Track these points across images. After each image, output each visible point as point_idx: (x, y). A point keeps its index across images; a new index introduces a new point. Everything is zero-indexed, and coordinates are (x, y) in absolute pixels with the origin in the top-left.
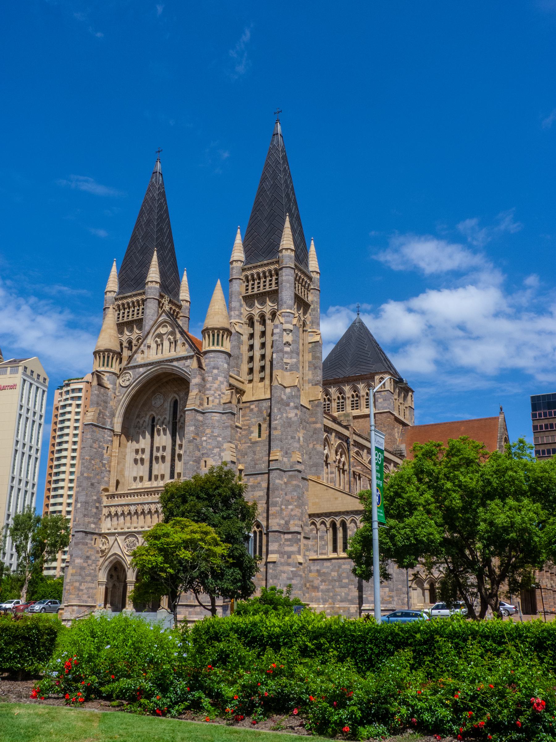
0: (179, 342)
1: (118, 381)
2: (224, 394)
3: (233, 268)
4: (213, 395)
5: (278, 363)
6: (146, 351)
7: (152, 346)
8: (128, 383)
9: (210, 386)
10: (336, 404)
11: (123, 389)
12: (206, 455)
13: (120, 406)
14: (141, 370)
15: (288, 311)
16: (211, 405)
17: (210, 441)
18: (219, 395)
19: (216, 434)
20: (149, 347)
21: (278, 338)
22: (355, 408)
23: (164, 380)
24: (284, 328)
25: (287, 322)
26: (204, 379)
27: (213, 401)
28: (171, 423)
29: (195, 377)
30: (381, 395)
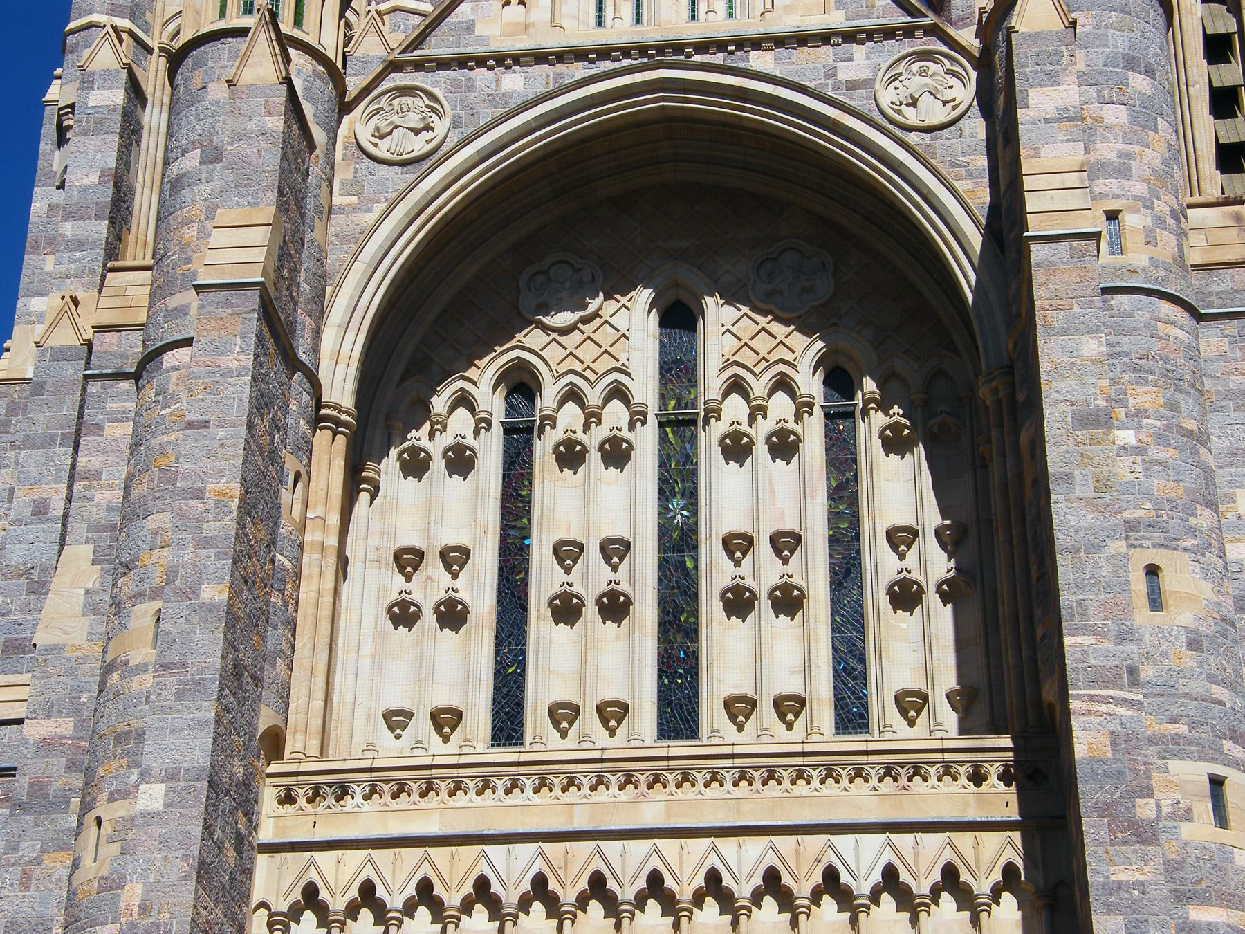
1: (343, 132)
8: (419, 146)
9: (1121, 154)
11: (382, 170)
12: (1157, 536)
13: (359, 268)
14: (515, 82)
17: (1167, 454)
18: (1174, 215)
19: (1191, 425)
28: (652, 421)
29: (1052, 79)
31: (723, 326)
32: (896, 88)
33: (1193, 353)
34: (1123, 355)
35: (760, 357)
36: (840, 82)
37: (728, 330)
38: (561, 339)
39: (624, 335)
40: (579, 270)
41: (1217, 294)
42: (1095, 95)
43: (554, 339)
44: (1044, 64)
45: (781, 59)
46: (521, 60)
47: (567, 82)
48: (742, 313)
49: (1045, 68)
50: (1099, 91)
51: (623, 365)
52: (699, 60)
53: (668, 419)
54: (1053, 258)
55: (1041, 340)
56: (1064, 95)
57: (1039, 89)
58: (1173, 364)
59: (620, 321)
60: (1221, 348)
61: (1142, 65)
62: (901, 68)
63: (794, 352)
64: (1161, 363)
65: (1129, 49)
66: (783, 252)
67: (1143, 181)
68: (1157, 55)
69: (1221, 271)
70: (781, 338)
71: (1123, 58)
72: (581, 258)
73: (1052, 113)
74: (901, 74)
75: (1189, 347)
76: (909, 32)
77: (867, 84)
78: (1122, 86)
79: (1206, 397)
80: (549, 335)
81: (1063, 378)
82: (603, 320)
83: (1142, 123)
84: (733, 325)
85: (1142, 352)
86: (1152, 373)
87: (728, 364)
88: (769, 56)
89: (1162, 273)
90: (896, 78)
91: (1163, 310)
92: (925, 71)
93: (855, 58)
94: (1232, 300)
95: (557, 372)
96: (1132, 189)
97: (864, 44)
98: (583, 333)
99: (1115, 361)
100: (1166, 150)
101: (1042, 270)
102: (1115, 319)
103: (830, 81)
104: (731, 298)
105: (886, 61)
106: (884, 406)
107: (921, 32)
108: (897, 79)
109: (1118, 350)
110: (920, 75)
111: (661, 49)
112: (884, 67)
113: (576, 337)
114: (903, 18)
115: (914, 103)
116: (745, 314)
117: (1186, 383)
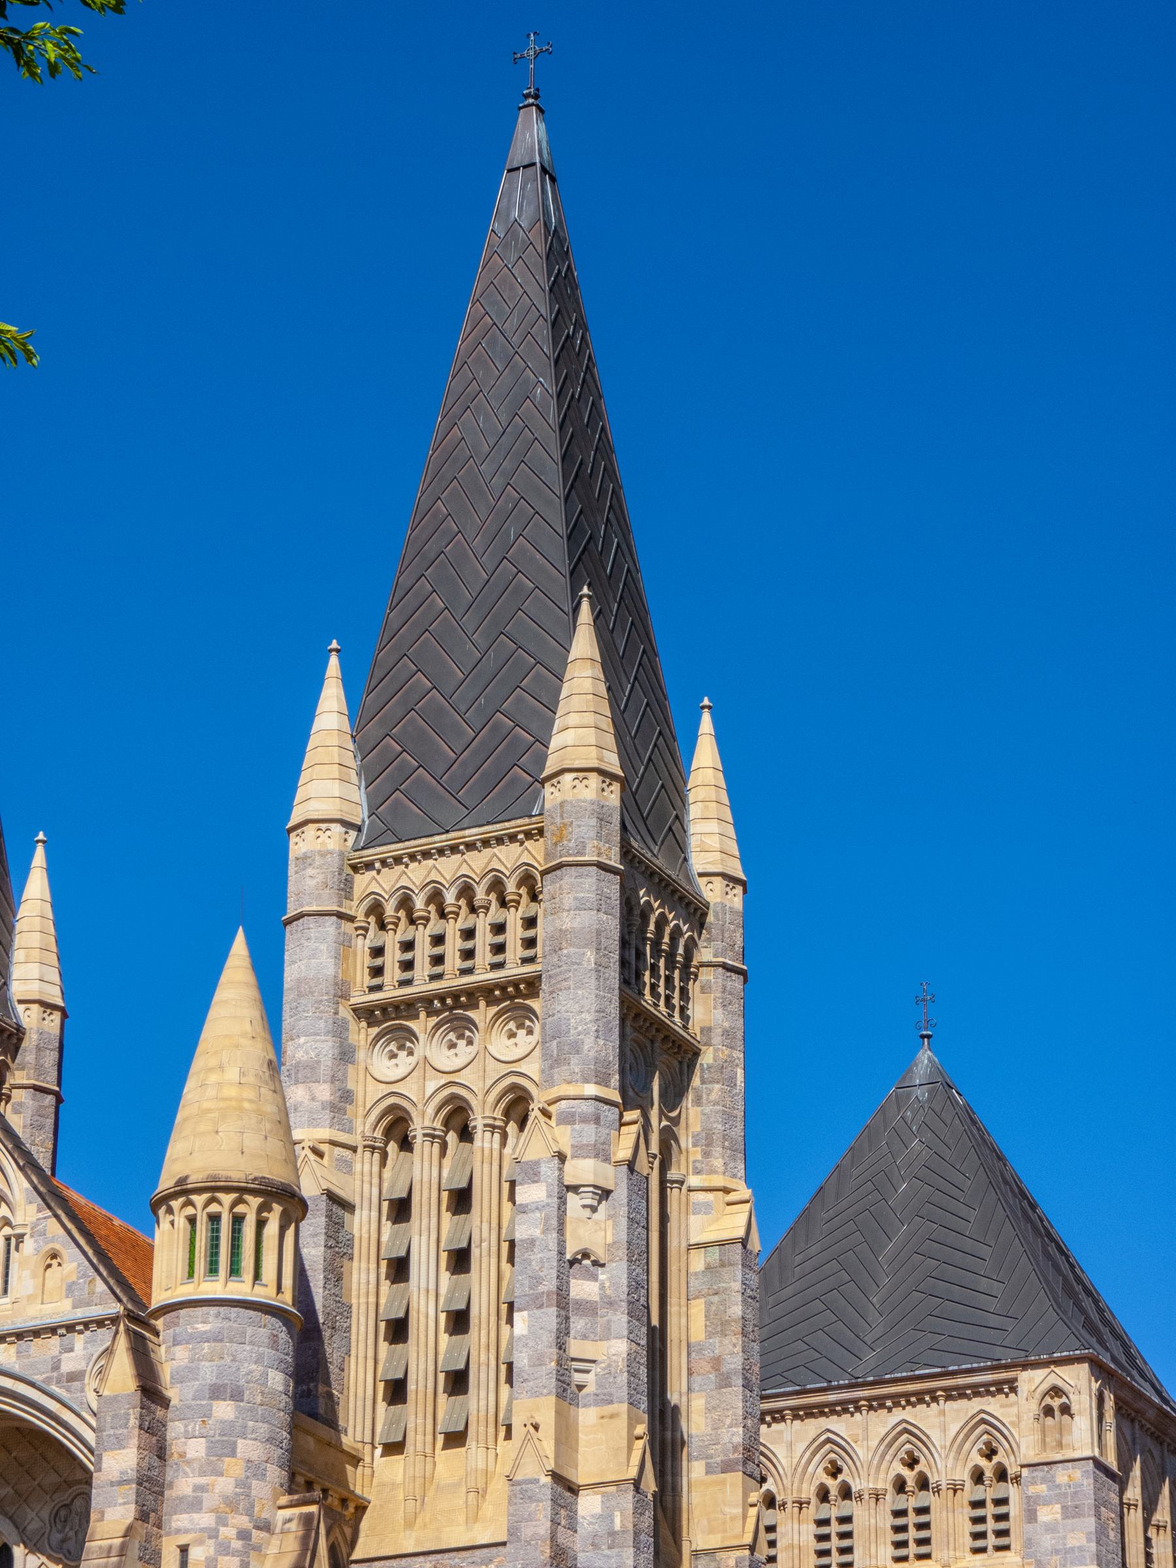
0: (28, 1245)
2: (266, 1527)
3: (304, 859)
5: (538, 1361)
9: (198, 1488)
10: (811, 1529)
15: (591, 1089)
18: (244, 1535)
21: (537, 1232)
22: (913, 1549)
25: (581, 1151)
26: (161, 1452)
29: (120, 1444)
30: (1050, 1481)
42: (182, 1430)
45: (21, 1353)
50: (186, 1426)
56: (126, 1459)
61: (229, 1391)
67: (212, 1511)
73: (115, 1476)
78: (207, 1415)
88: (13, 1349)
93: (76, 1348)
103: (55, 1374)
104: (34, 1547)
105: (96, 1351)
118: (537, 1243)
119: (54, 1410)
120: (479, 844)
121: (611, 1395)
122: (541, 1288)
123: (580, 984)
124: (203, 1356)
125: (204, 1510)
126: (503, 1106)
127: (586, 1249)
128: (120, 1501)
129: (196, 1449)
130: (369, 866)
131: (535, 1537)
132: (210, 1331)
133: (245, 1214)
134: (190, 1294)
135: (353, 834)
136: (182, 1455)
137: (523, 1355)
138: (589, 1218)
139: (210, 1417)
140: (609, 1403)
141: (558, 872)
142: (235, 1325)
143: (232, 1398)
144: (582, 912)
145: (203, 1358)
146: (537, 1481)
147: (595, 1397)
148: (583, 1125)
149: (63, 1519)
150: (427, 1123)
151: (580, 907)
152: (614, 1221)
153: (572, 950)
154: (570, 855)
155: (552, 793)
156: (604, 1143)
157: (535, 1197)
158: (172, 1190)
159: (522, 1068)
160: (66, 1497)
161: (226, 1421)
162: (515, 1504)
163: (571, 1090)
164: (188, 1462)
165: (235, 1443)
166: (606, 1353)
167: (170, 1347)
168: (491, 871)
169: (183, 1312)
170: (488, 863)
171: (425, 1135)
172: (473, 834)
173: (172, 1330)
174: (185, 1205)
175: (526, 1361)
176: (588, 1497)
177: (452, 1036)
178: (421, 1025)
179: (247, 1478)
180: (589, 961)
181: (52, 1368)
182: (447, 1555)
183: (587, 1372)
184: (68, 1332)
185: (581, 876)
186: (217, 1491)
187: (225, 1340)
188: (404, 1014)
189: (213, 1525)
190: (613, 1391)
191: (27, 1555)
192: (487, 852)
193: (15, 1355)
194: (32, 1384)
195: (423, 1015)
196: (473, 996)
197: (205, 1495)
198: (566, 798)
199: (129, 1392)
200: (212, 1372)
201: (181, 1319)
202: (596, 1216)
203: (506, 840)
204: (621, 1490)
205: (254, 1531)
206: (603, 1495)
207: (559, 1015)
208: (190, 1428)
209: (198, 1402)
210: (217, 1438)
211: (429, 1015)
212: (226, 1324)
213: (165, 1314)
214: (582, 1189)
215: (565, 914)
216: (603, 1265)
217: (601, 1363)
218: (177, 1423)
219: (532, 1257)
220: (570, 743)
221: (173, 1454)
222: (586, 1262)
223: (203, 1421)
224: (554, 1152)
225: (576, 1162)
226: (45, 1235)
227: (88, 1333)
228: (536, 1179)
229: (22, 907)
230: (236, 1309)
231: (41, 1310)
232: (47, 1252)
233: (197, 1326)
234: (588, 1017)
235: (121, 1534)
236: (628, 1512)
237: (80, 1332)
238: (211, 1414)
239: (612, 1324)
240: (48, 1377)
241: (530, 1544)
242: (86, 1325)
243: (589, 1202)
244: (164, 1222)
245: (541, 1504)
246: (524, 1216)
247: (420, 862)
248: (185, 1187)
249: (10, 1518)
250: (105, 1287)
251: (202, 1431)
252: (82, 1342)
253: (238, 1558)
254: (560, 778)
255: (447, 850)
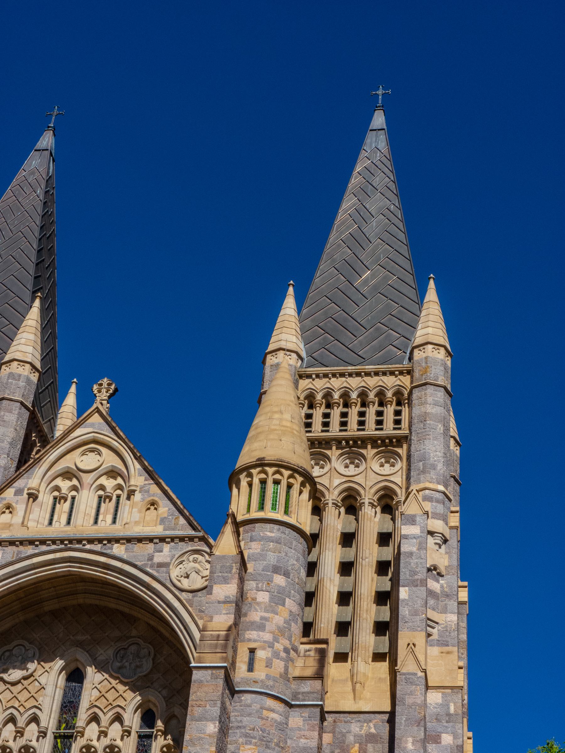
0: (138, 497)
4: (271, 646)
5: (415, 613)
6: (20, 509)
7: (41, 496)
9: (262, 618)
15: (441, 488)
16: (260, 673)
18: (286, 650)
20: (33, 497)
21: (414, 549)
23: (48, 607)
24: (430, 529)
25: (436, 516)
27: (269, 665)
29: (226, 581)
31: (93, 684)
32: (180, 568)
33: (283, 727)
34: (242, 727)
35: (109, 703)
36: (154, 563)
37: (96, 687)
38: (12, 688)
39: (43, 688)
40: (28, 650)
41: (303, 693)
42: (255, 586)
43: (8, 688)
44: (224, 572)
46: (2, 543)
47: (23, 556)
48: (104, 678)
49: (223, 574)
50: (257, 584)
51: (40, 704)
52: (89, 548)
53: (60, 734)
54: (203, 679)
55: (188, 722)
56: (229, 590)
57: (218, 585)
58: (267, 734)
59: (43, 680)
60: (299, 723)
61: (283, 571)
62: (184, 558)
63: (126, 701)
64: (261, 732)
65: (277, 562)
66: (130, 645)
67: (271, 633)
68: (293, 565)
69: (306, 681)
70: (121, 692)
71: (272, 567)
72: (30, 644)
73: (222, 598)
74: (184, 561)
75: (280, 723)
76: (191, 539)
77: (165, 565)
78: (270, 581)
79: (287, 750)
80: (6, 686)
81: (194, 745)
82: (34, 678)
83: (276, 602)
84: (99, 684)
85: (252, 726)
86: (255, 738)
87: (93, 706)
88: (123, 547)
89: (271, 683)
90: (181, 563)
91: (268, 703)
92: (195, 560)
94: (309, 697)
95: (6, 707)
96: (264, 637)
97: (169, 543)
98: (23, 685)
99: (238, 731)
100: (288, 616)
101: (196, 684)
102: (242, 707)
103: (150, 563)
104: (101, 667)
106: (165, 733)
107: (197, 540)
108: (182, 563)
109: (240, 724)
110: (193, 562)
111: (71, 541)
112: (177, 556)
113: (20, 687)
114: (190, 531)
115: (187, 577)
116: (106, 679)
117: (273, 744)
118: (415, 554)
119: (147, 581)
120: (372, 374)
121: (447, 642)
122: (416, 577)
123: (435, 438)
124: (270, 549)
125: (266, 631)
126: (378, 496)
127: (436, 565)
128: (224, 612)
129: (263, 597)
130: (309, 376)
131: (414, 704)
132: (274, 537)
133: (294, 484)
134: (263, 516)
135: (300, 362)
136: (254, 599)
137: (405, 609)
138: (438, 550)
139: (272, 581)
140: (446, 646)
141: (424, 387)
142: (288, 537)
143: (284, 575)
144: (436, 407)
145: (270, 550)
146: (416, 674)
147: (437, 642)
148: (437, 504)
149: (121, 656)
150: (334, 498)
151: (436, 404)
152: (449, 555)
153: (432, 422)
154: (431, 380)
155: (419, 354)
156: (446, 516)
157: (413, 532)
158: (255, 463)
159: (392, 478)
160: (125, 644)
161: (280, 586)
162: (402, 685)
163: (431, 486)
164: (258, 604)
165: (285, 599)
166: (444, 620)
167: (248, 542)
168: (379, 386)
169: (257, 525)
170: (377, 383)
171: (333, 504)
172: (370, 368)
173: (249, 534)
174: (260, 472)
175: (407, 612)
176: (433, 693)
177: (348, 461)
178: (334, 453)
179: (290, 620)
180: (440, 429)
181: (148, 559)
182: (342, 715)
183: (433, 628)
184: (160, 542)
185: (436, 391)
186: (274, 622)
187: (282, 544)
188: (323, 446)
189: (271, 640)
190: (449, 639)
191: (95, 673)
192: (377, 378)
193: (124, 550)
194: (135, 566)
195: (334, 448)
196: (363, 442)
197: (267, 623)
198: (429, 355)
199: (233, 554)
200: (274, 558)
201: (256, 529)
202: (440, 550)
203: (388, 373)
204: (454, 692)
205: (291, 650)
206: (443, 693)
207: (424, 451)
208: (260, 585)
209: (265, 573)
210: (276, 594)
211: (337, 449)
212: (283, 536)
213: (244, 525)
214: (436, 534)
215: (428, 406)
216: (442, 576)
217: (441, 624)
218: (251, 582)
219: (411, 561)
220: (430, 333)
221: (248, 598)
222: (434, 572)
223: (268, 583)
224: (425, 511)
225: (433, 520)
226: (149, 492)
227: (172, 544)
228: (414, 523)
229: (62, 408)
230: (289, 529)
231: (143, 529)
232: (149, 501)
233: (267, 533)
234: (440, 454)
235: (225, 629)
236: (458, 704)
237: (168, 543)
238: (273, 580)
239: (448, 606)
240: (145, 564)
241: (411, 708)
242: (173, 539)
243: (439, 542)
244: (243, 481)
245: (418, 687)
246: (407, 540)
247: (337, 378)
248: (263, 462)
249: (87, 652)
250: (186, 522)
251: (268, 588)
252: (169, 548)
253: (284, 663)
254: (425, 347)
255: (354, 374)
